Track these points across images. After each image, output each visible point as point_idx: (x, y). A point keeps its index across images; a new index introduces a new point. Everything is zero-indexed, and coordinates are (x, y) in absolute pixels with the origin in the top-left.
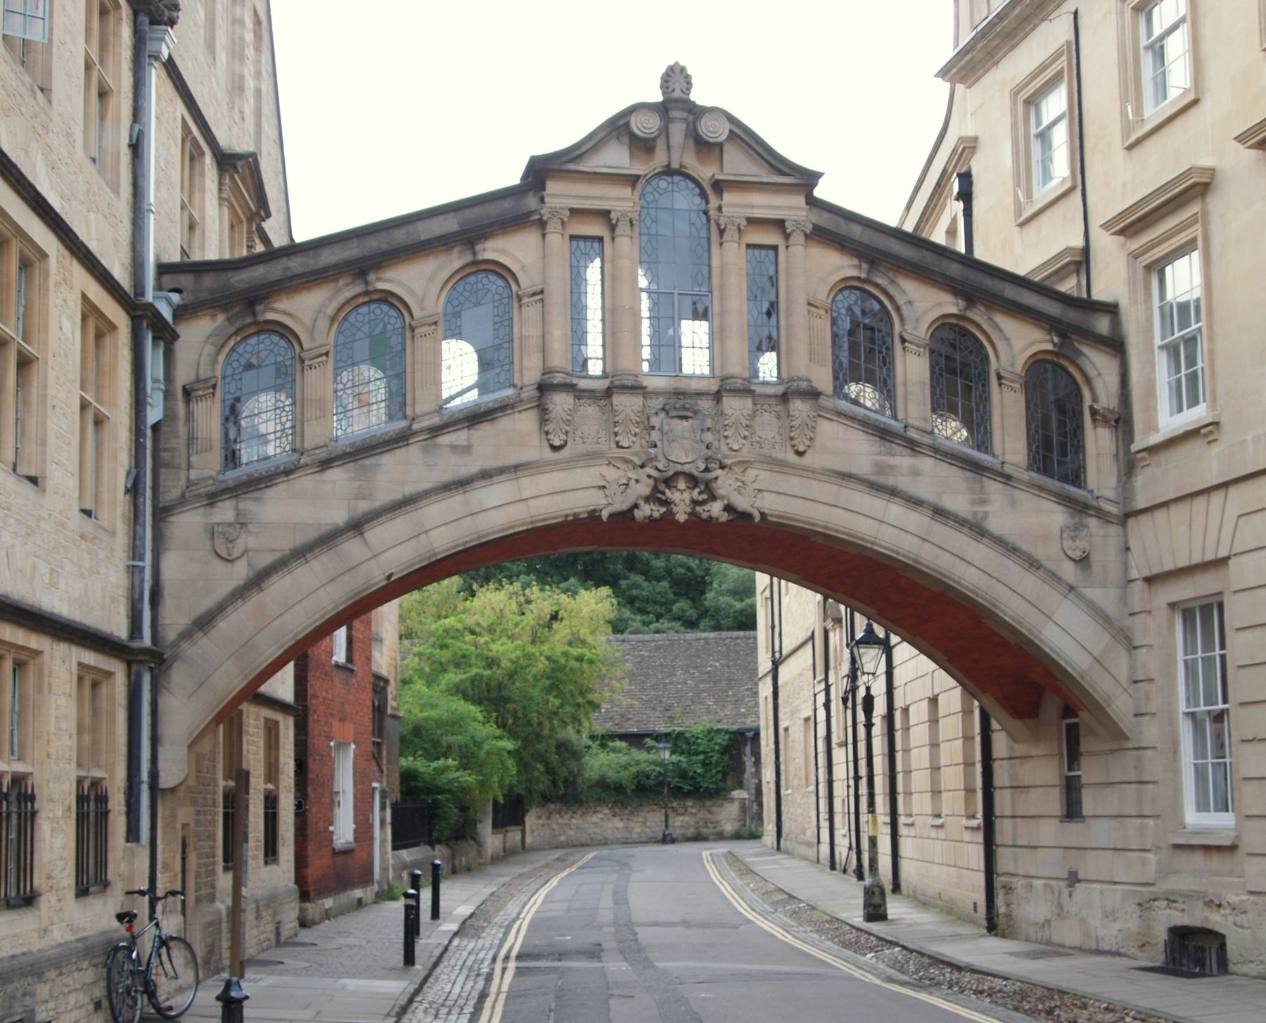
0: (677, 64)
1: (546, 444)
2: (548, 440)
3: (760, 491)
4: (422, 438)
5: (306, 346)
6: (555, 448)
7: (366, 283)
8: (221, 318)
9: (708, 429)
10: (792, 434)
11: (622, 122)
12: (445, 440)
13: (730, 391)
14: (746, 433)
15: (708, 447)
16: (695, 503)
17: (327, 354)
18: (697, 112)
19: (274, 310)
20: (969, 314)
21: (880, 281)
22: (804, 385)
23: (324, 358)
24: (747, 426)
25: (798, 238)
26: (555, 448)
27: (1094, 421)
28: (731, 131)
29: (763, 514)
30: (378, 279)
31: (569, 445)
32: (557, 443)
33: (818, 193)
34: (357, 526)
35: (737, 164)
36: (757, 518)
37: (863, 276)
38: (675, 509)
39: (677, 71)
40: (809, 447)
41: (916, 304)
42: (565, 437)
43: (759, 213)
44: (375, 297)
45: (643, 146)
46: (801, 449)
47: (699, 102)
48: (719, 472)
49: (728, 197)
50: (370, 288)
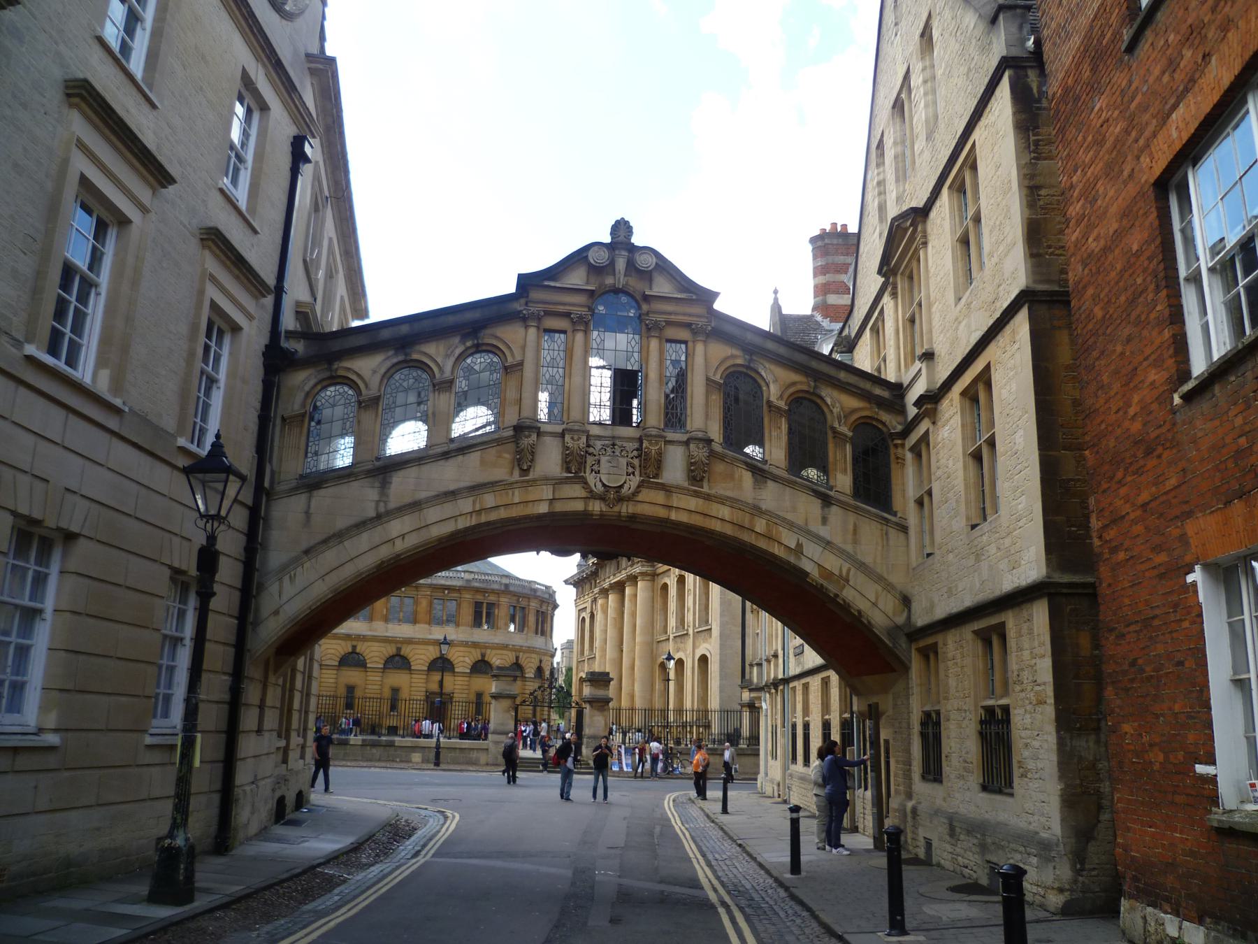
0: (623, 218)
7: (406, 355)
11: (585, 255)
18: (633, 249)
22: (700, 435)
28: (656, 264)
32: (525, 468)
33: (718, 306)
34: (380, 518)
35: (661, 287)
39: (622, 223)
43: (673, 318)
44: (411, 364)
45: (596, 270)
47: (636, 244)
50: (408, 358)
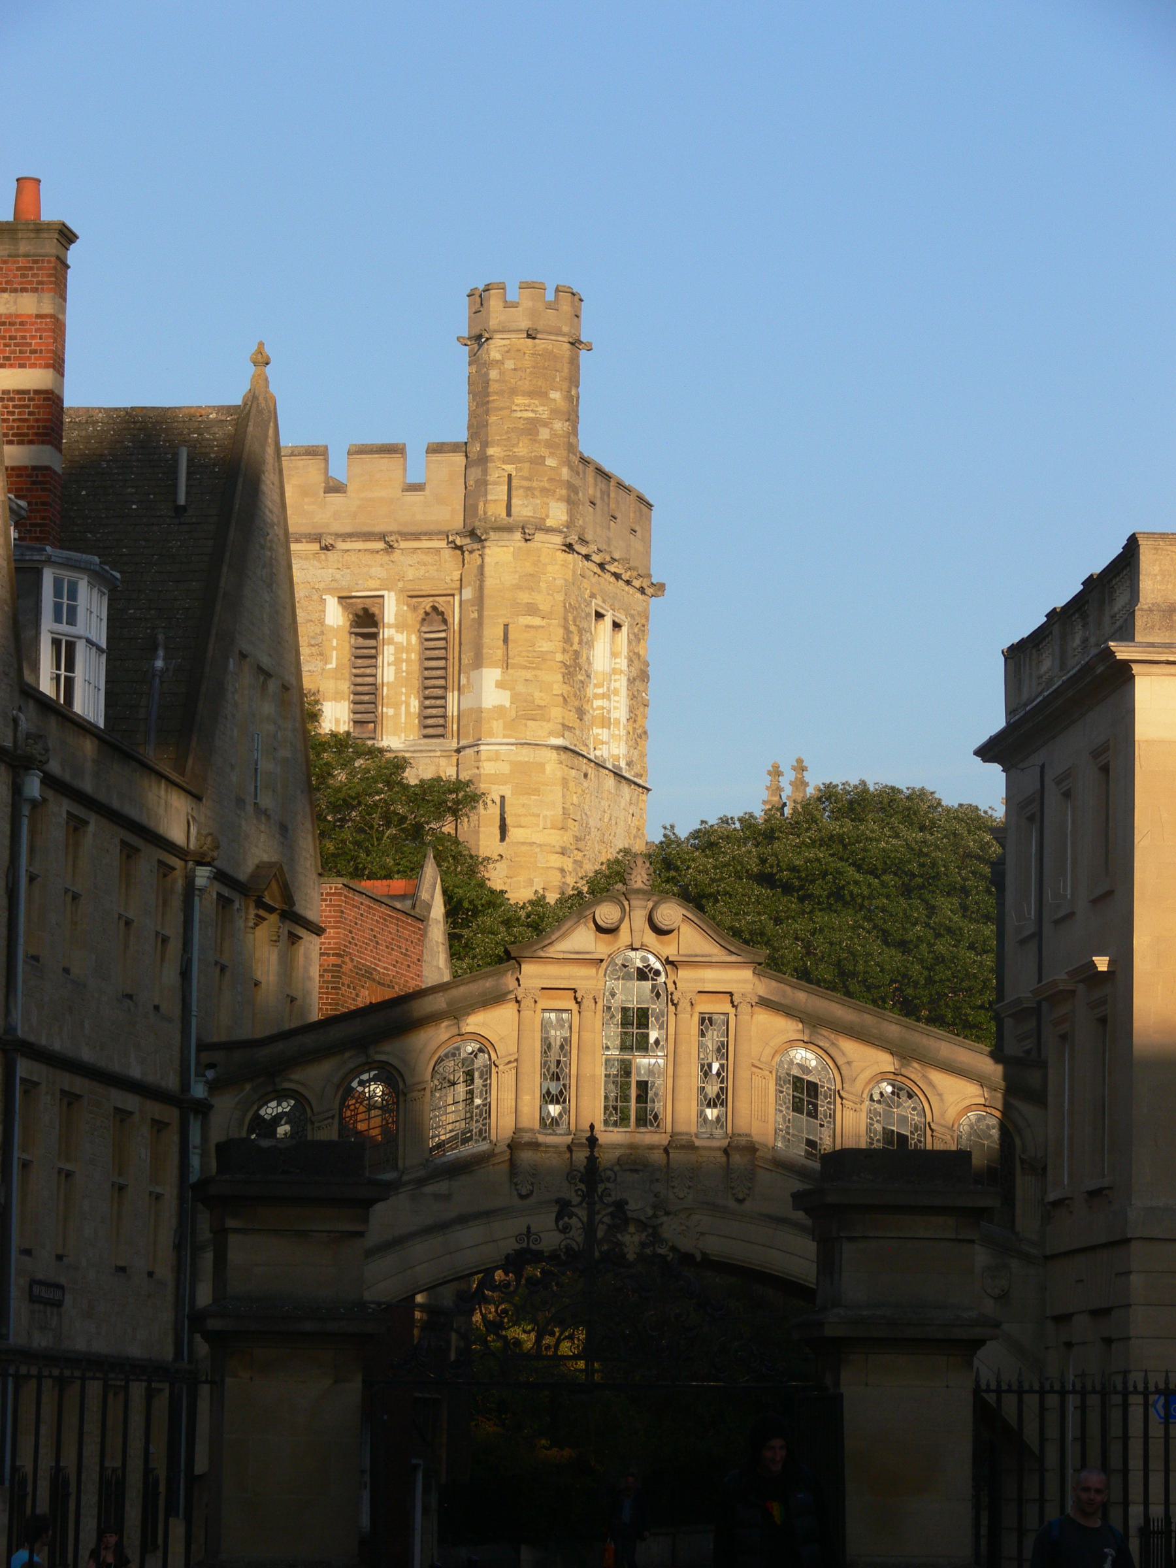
1: (515, 1193)
2: (517, 1190)
3: (702, 1234)
4: (410, 1188)
5: (315, 1110)
6: (522, 1197)
8: (248, 1087)
9: (657, 1180)
10: (733, 1185)
12: (429, 1189)
13: (676, 1147)
14: (690, 1184)
15: (655, 1196)
16: (643, 1245)
17: (333, 1117)
19: (291, 1081)
20: (903, 1071)
21: (821, 1044)
23: (330, 1120)
24: (691, 1178)
25: (744, 1008)
26: (522, 1197)
27: (1023, 1168)
29: (704, 1254)
30: (377, 1053)
31: (534, 1194)
32: (524, 1192)
36: (699, 1259)
37: (806, 1039)
38: (626, 1250)
40: (748, 1195)
41: (855, 1064)
42: (531, 1188)
46: (741, 1196)
48: (665, 1219)
49: (684, 973)
50: (369, 1060)
